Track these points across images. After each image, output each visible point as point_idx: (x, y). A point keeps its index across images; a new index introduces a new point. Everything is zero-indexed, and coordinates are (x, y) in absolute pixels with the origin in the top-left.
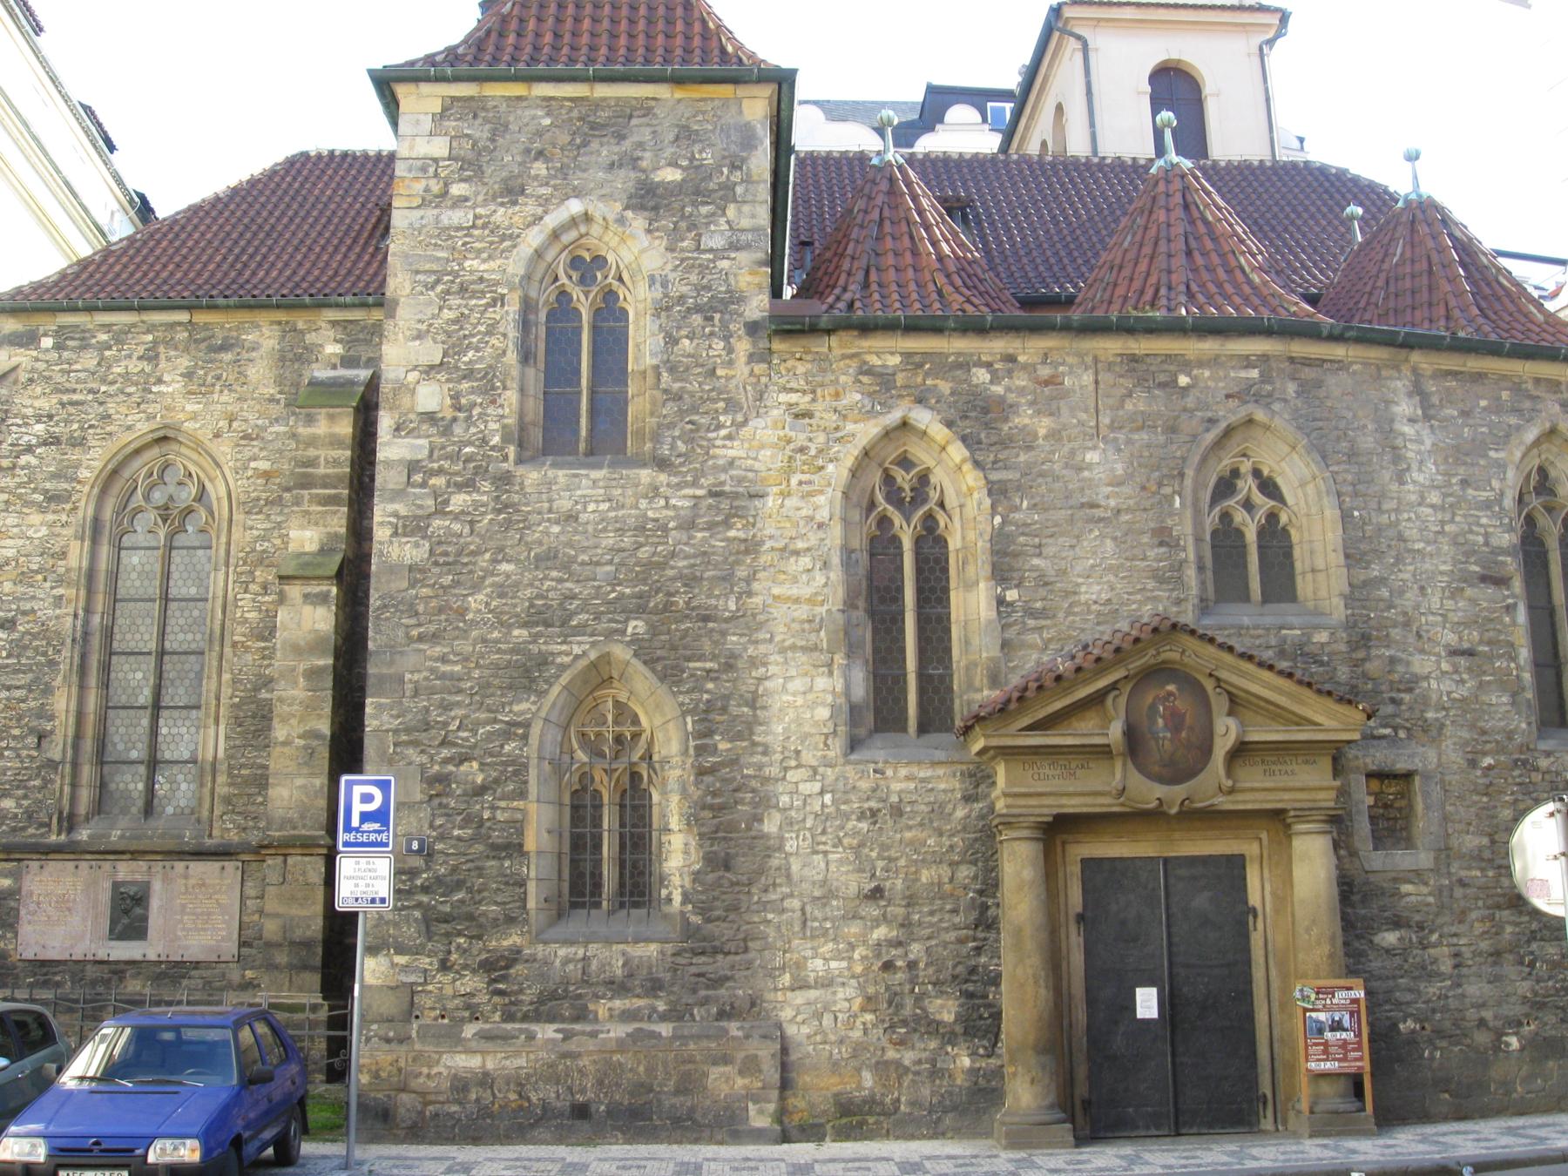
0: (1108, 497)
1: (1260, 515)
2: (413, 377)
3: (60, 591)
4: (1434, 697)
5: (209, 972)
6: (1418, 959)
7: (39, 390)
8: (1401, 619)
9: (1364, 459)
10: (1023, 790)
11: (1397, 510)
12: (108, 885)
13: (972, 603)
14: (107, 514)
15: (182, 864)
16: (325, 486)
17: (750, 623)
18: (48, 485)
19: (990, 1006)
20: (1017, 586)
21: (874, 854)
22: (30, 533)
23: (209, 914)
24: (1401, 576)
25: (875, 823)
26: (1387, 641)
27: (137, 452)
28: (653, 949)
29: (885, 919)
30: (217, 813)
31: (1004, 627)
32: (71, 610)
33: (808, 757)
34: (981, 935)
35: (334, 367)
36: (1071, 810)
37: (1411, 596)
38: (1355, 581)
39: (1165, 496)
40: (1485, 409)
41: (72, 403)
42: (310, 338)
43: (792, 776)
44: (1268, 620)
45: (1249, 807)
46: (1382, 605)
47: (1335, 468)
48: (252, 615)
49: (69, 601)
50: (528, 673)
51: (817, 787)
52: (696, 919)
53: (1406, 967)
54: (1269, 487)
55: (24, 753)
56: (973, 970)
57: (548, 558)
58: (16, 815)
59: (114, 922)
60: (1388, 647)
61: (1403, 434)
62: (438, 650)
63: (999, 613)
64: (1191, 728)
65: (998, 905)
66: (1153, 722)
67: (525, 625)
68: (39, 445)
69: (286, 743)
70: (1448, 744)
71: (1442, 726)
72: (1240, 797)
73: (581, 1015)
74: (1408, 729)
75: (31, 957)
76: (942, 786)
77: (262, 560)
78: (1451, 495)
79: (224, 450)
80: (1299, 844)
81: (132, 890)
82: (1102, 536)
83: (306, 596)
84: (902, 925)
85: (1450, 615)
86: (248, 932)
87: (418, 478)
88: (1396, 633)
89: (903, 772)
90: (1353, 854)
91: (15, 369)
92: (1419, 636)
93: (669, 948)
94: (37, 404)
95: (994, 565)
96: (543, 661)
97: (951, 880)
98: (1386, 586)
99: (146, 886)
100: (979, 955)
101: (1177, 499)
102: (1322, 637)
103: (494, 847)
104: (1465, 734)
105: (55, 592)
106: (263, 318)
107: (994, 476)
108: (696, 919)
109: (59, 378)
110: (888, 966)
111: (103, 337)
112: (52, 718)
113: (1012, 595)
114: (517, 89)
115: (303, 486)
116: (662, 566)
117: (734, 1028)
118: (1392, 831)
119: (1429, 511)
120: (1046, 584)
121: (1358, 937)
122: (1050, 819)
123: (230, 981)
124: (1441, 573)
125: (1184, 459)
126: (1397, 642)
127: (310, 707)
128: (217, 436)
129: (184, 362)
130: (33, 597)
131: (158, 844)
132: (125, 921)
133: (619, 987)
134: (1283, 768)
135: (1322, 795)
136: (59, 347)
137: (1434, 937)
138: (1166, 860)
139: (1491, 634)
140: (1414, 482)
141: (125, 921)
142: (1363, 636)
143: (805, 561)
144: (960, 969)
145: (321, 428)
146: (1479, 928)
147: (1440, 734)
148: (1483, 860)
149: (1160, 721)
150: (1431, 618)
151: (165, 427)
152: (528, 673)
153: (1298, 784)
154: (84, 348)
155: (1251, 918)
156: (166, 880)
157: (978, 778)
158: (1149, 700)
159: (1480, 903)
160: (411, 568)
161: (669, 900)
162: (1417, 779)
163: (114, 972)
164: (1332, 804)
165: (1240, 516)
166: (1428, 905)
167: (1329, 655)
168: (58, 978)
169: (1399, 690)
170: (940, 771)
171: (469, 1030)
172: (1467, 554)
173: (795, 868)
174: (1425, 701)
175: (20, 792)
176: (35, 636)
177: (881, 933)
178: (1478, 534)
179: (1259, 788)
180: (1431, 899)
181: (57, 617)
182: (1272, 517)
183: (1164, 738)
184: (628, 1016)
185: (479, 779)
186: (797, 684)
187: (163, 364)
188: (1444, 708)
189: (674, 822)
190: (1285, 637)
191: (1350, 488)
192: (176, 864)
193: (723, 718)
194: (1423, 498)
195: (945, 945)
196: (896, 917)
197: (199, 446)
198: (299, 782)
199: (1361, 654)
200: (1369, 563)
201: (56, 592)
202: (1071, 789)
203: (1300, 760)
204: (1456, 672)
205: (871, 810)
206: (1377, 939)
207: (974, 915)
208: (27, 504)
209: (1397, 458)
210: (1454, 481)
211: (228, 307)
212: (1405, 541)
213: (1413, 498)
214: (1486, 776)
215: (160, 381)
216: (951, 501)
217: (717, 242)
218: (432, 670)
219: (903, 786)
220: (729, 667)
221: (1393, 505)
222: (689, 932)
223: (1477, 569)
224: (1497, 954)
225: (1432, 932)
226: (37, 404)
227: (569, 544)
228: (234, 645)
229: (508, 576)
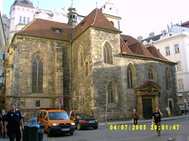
2: (95, 55)
3: (28, 68)
7: (24, 45)
13: (134, 78)
14: (32, 60)
16: (60, 60)
17: (121, 79)
18: (26, 56)
22: (24, 61)
27: (35, 53)
28: (115, 106)
30: (47, 93)
32: (29, 70)
33: (125, 90)
35: (56, 46)
41: (28, 47)
42: (54, 43)
43: (124, 92)
44: (153, 81)
48: (49, 72)
49: (29, 69)
50: (105, 82)
51: (126, 92)
52: (118, 103)
54: (151, 70)
55: (25, 86)
57: (106, 72)
58: (24, 93)
62: (98, 80)
67: (105, 78)
68: (24, 51)
69: (59, 86)
73: (111, 111)
77: (50, 66)
79: (45, 54)
80: (156, 98)
81: (38, 101)
83: (60, 71)
86: (51, 106)
87: (96, 64)
89: (131, 91)
91: (21, 41)
93: (117, 106)
94: (24, 46)
96: (106, 81)
99: (39, 101)
102: (156, 82)
103: (104, 97)
105: (27, 68)
106: (49, 40)
107: (137, 68)
108: (118, 103)
109: (26, 44)
110: (131, 107)
111: (31, 40)
112: (28, 82)
114: (101, 29)
115: (58, 60)
116: (115, 74)
117: (121, 112)
127: (61, 83)
128: (45, 52)
129: (40, 44)
130: (25, 69)
131: (41, 97)
132: (38, 105)
133: (113, 109)
136: (26, 40)
141: (38, 105)
143: (124, 74)
145: (59, 54)
146: (164, 104)
151: (39, 51)
152: (105, 82)
154: (29, 40)
157: (136, 92)
160: (96, 72)
161: (116, 102)
170: (134, 91)
171: (103, 113)
173: (125, 99)
175: (24, 90)
176: (25, 73)
177: (130, 104)
179: (154, 94)
181: (28, 71)
184: (114, 111)
185: (102, 91)
186: (124, 84)
187: (38, 44)
189: (116, 95)
193: (119, 87)
197: (42, 53)
198: (60, 90)
201: (27, 68)
208: (23, 58)
211: (46, 38)
215: (38, 46)
216: (132, 69)
217: (116, 46)
218: (98, 82)
220: (120, 83)
222: (118, 104)
226: (24, 46)
227: (108, 71)
228: (48, 75)
229: (103, 74)
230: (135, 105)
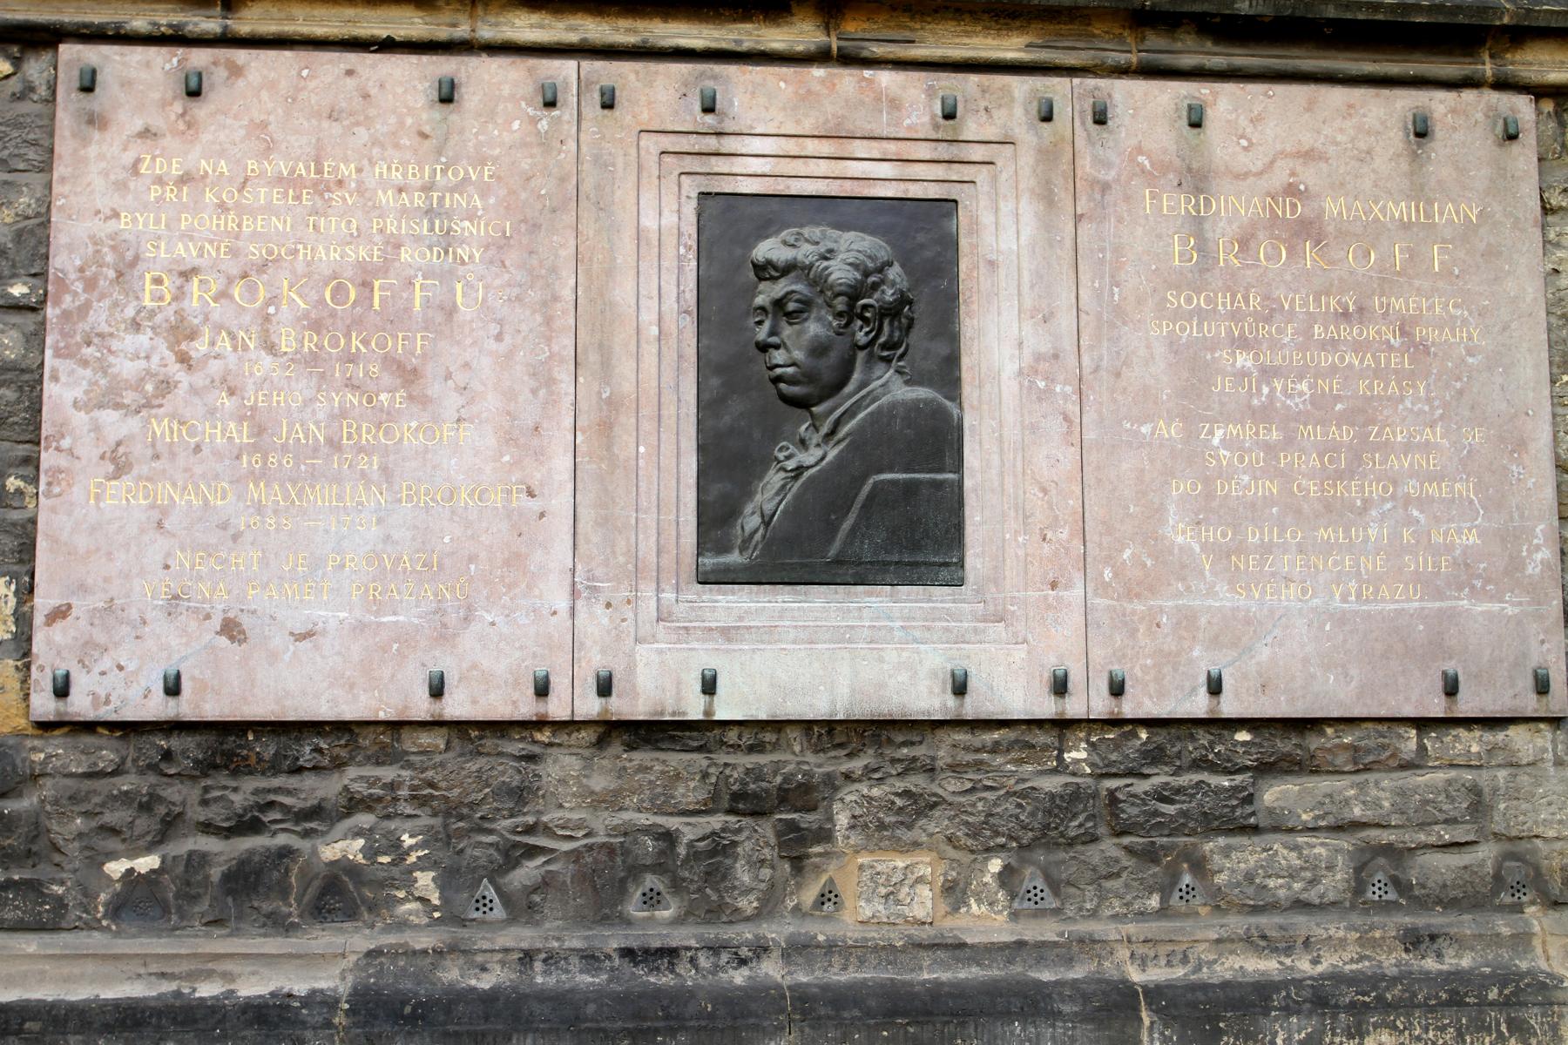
5: (1383, 789)
12: (668, 216)
15: (1169, 95)
23: (1361, 415)
59: (725, 466)
75: (156, 708)
81: (847, 253)
99: (924, 235)
123: (1516, 847)
156: (1066, 193)
163: (746, 802)
168: (341, 847)
192: (1125, 94)
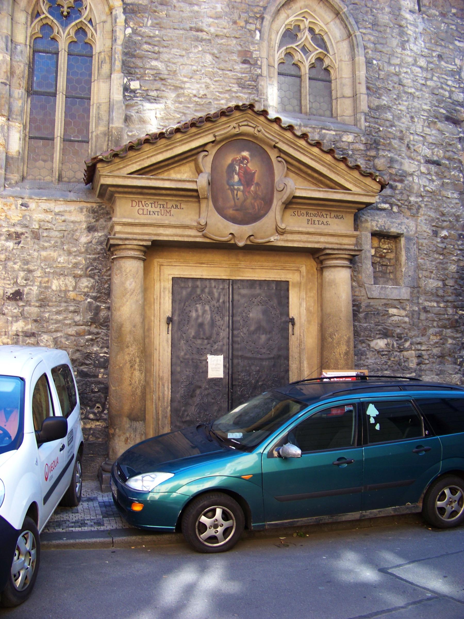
0: (210, 26)
1: (312, 58)
4: (416, 187)
6: (397, 359)
8: (398, 134)
9: (382, 29)
10: (130, 220)
11: (400, 66)
19: (100, 383)
20: (138, 79)
21: (16, 267)
24: (400, 107)
25: (19, 243)
26: (389, 147)
29: (23, 316)
31: (127, 106)
34: (95, 330)
36: (166, 238)
37: (406, 120)
38: (372, 105)
39: (250, 31)
40: (454, 14)
45: (296, 245)
46: (388, 124)
47: (364, 31)
53: (389, 363)
54: (319, 41)
56: (88, 356)
60: (389, 151)
61: (406, 19)
63: (124, 96)
64: (257, 184)
65: (109, 308)
66: (230, 177)
70: (421, 219)
71: (420, 207)
72: (290, 237)
74: (399, 207)
76: (73, 218)
78: (431, 63)
80: (329, 274)
82: (204, 52)
84: (36, 321)
85: (428, 137)
88: (395, 143)
90: (361, 285)
92: (408, 147)
95: (124, 63)
97: (75, 288)
98: (390, 111)
100: (93, 345)
101: (258, 32)
102: (349, 138)
104: (433, 215)
113: (135, 85)
118: (384, 273)
119: (419, 70)
120: (162, 79)
121: (362, 342)
122: (149, 243)
124: (424, 110)
125: (265, 8)
126: (395, 149)
134: (322, 219)
135: (346, 241)
137: (407, 345)
138: (234, 282)
139: (450, 153)
140: (411, 50)
142: (375, 141)
144: (77, 355)
146: (435, 339)
147: (418, 213)
148: (438, 296)
149: (236, 178)
150: (416, 137)
153: (331, 232)
155: (290, 326)
158: (229, 161)
159: (435, 324)
162: (403, 240)
164: (352, 247)
165: (298, 56)
166: (405, 323)
167: (353, 150)
169: (395, 181)
172: (439, 102)
174: (409, 190)
178: (445, 90)
180: (407, 319)
182: (320, 60)
183: (238, 190)
188: (421, 196)
190: (325, 135)
191: (372, 45)
194: (415, 61)
195: (68, 336)
196: (30, 314)
199: (373, 153)
200: (381, 95)
202: (167, 222)
203: (332, 215)
204: (429, 174)
205: (16, 233)
206: (373, 344)
207: (89, 316)
209: (402, 33)
210: (434, 54)
212: (404, 86)
213: (410, 60)
214: (443, 242)
219: (42, 216)
221: (397, 61)
223: (444, 112)
224: (442, 356)
225: (406, 341)
230: (78, 334)
